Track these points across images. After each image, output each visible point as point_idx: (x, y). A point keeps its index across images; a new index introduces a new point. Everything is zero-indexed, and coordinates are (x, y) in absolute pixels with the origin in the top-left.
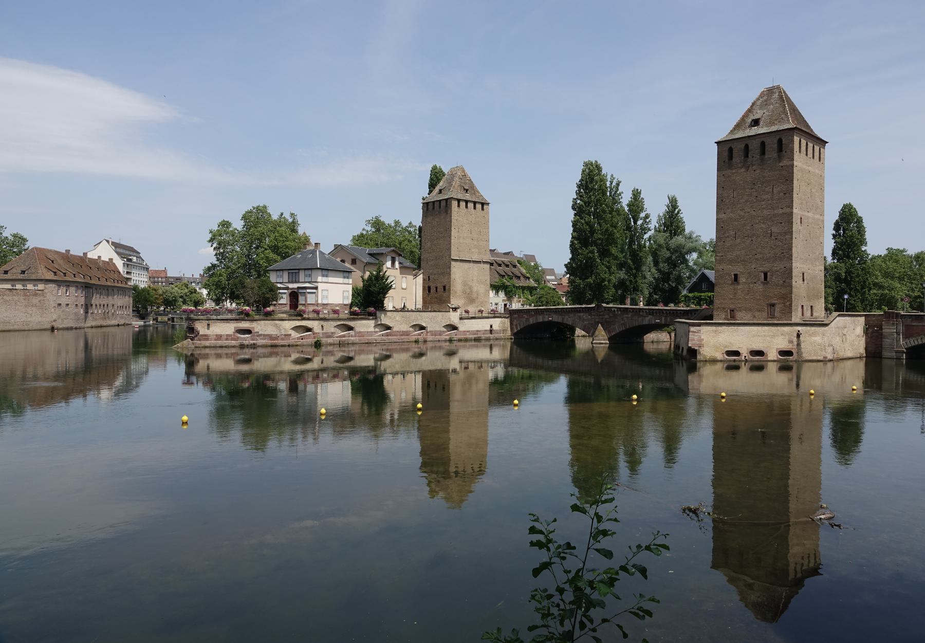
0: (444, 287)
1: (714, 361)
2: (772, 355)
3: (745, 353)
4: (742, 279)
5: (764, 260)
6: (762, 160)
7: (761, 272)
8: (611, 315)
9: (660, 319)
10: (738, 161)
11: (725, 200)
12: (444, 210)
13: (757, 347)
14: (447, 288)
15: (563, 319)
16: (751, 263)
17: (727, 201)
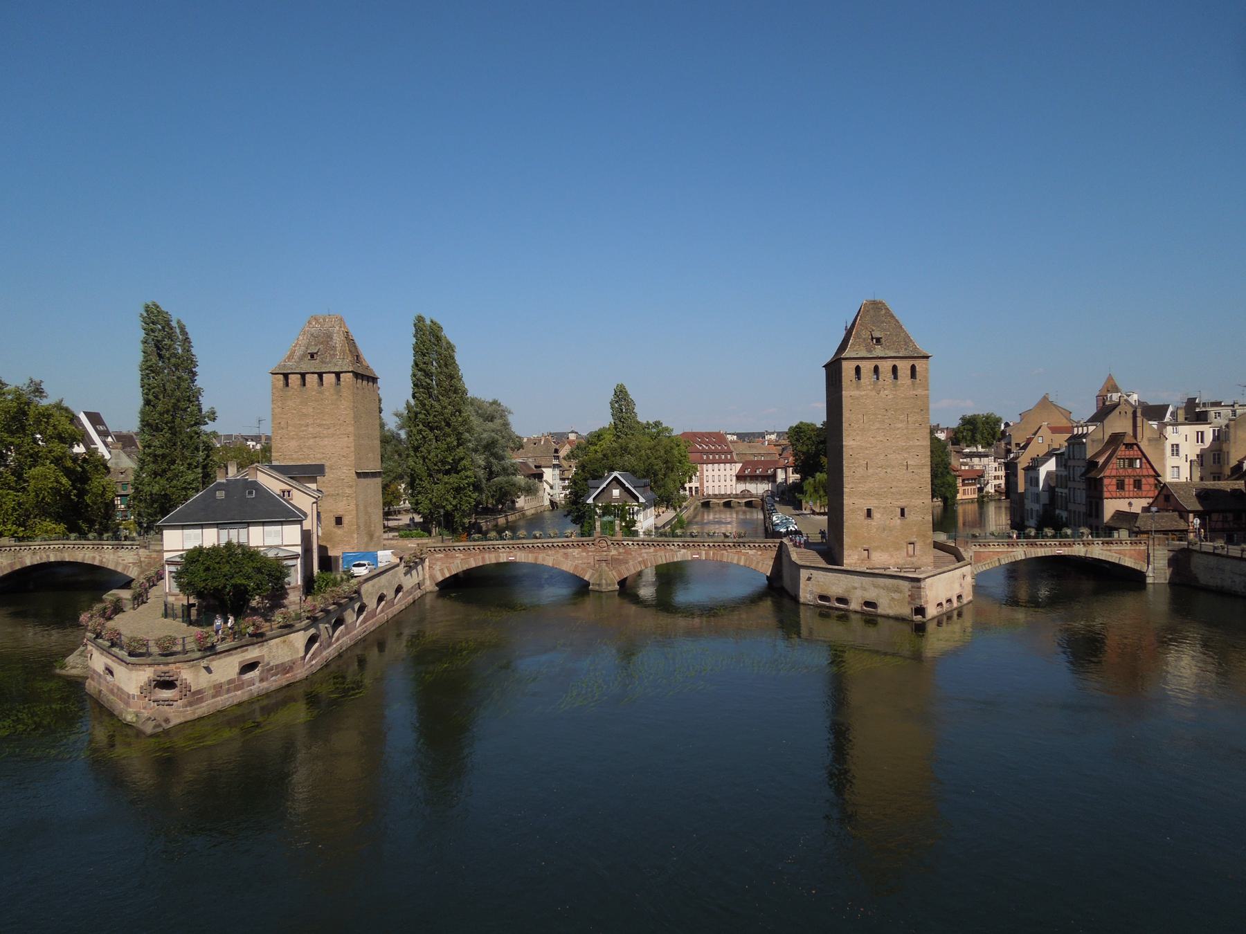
0: (339, 521)
1: (933, 618)
2: (955, 604)
3: (944, 603)
4: (876, 515)
5: (901, 495)
6: (895, 385)
7: (898, 507)
8: (621, 550)
10: (868, 383)
11: (852, 424)
12: (332, 391)
13: (949, 597)
14: (345, 520)
15: (536, 558)
16: (886, 497)
17: (857, 426)
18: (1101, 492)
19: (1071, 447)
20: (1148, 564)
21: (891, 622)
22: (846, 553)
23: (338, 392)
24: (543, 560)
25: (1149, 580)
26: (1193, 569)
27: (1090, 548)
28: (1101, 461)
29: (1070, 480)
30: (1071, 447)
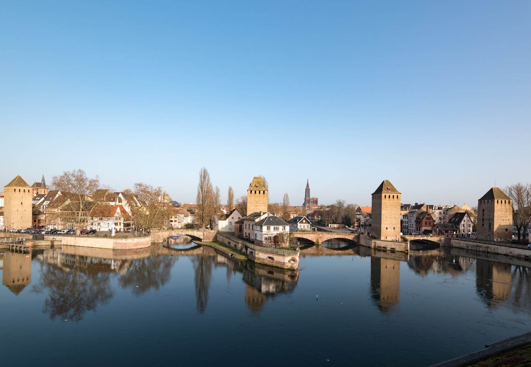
4: (388, 228)
8: (322, 235)
9: (340, 236)
12: (262, 195)
15: (302, 236)
18: (422, 225)
19: (410, 214)
20: (440, 242)
21: (400, 252)
22: (381, 237)
23: (264, 196)
24: (304, 237)
25: (440, 245)
26: (451, 243)
27: (428, 238)
28: (421, 218)
29: (409, 222)
30: (410, 214)
